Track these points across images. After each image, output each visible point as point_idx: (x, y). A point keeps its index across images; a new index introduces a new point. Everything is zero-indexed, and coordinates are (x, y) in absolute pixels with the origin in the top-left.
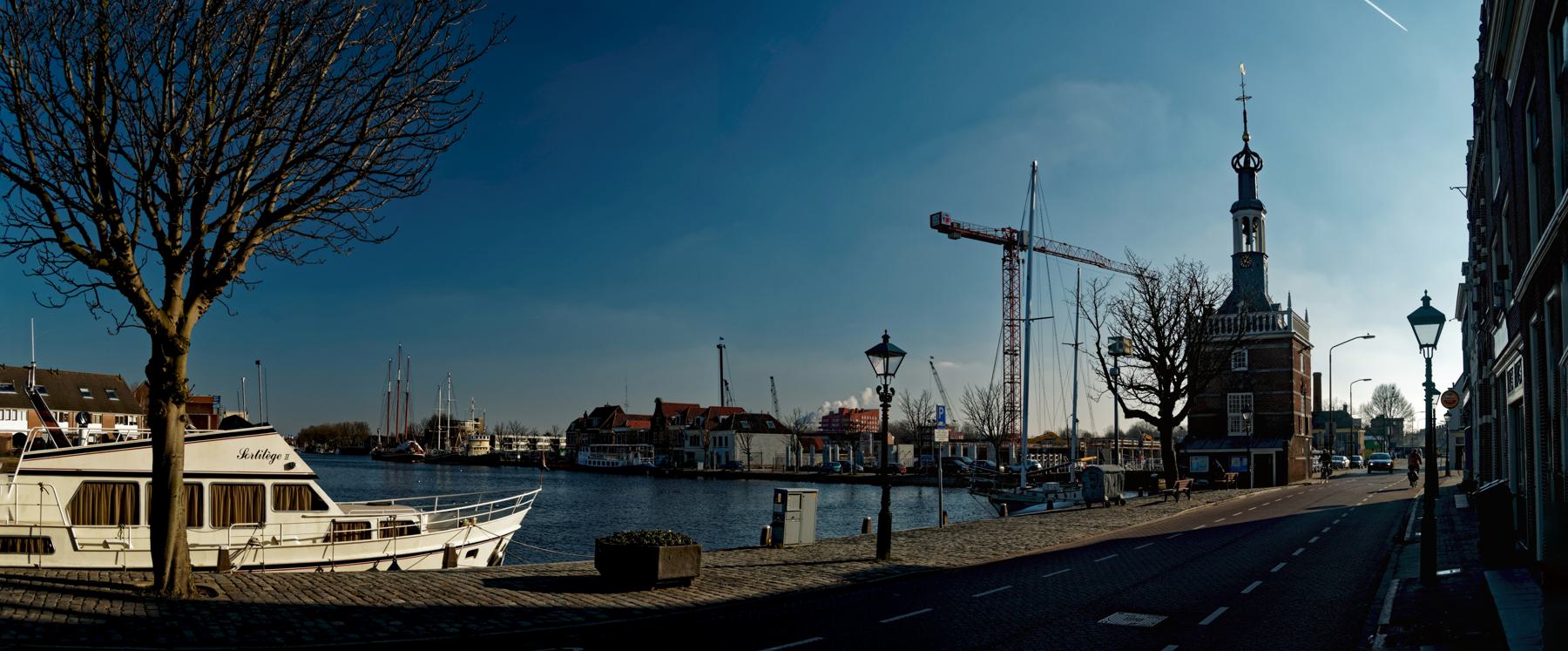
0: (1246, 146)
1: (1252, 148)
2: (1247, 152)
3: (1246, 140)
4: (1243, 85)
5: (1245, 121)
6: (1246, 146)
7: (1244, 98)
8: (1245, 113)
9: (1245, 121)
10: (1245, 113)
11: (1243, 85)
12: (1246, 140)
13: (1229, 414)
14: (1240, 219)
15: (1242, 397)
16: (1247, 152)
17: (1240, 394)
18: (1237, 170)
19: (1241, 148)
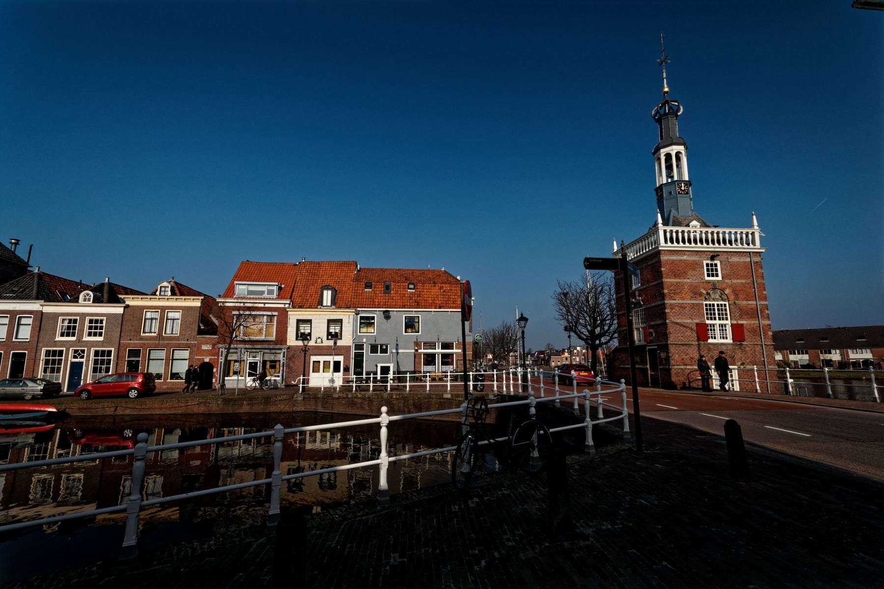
15: (718, 305)
17: (716, 303)
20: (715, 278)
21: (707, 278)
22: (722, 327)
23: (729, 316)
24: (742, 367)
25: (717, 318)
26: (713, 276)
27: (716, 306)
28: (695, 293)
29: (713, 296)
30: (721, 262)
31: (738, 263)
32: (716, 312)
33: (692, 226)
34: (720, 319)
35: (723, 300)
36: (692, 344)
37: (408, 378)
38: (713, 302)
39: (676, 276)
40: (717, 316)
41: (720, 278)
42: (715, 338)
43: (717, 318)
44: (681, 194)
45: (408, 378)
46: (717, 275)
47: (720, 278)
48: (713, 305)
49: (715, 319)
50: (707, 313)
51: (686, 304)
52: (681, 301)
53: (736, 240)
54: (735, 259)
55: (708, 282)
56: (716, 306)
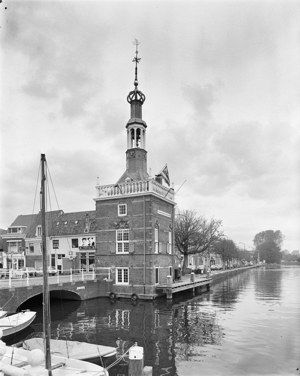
0: (136, 88)
1: (139, 88)
2: (136, 92)
3: (136, 84)
4: (137, 52)
5: (136, 74)
7: (137, 60)
8: (136, 69)
9: (136, 74)
10: (136, 69)
11: (137, 52)
12: (136, 84)
13: (117, 242)
14: (129, 130)
15: (124, 231)
16: (136, 92)
17: (123, 230)
18: (131, 102)
19: (133, 88)
21: (119, 215)
24: (131, 268)
25: (123, 239)
26: (122, 214)
27: (123, 231)
28: (111, 225)
29: (121, 226)
30: (127, 204)
31: (137, 203)
33: (127, 181)
34: (124, 240)
35: (127, 228)
36: (107, 255)
39: (102, 216)
40: (123, 238)
41: (126, 215)
42: (122, 251)
43: (123, 239)
49: (121, 240)
50: (128, 236)
51: (106, 232)
52: (103, 230)
54: (134, 202)
55: (119, 218)
56: (123, 231)
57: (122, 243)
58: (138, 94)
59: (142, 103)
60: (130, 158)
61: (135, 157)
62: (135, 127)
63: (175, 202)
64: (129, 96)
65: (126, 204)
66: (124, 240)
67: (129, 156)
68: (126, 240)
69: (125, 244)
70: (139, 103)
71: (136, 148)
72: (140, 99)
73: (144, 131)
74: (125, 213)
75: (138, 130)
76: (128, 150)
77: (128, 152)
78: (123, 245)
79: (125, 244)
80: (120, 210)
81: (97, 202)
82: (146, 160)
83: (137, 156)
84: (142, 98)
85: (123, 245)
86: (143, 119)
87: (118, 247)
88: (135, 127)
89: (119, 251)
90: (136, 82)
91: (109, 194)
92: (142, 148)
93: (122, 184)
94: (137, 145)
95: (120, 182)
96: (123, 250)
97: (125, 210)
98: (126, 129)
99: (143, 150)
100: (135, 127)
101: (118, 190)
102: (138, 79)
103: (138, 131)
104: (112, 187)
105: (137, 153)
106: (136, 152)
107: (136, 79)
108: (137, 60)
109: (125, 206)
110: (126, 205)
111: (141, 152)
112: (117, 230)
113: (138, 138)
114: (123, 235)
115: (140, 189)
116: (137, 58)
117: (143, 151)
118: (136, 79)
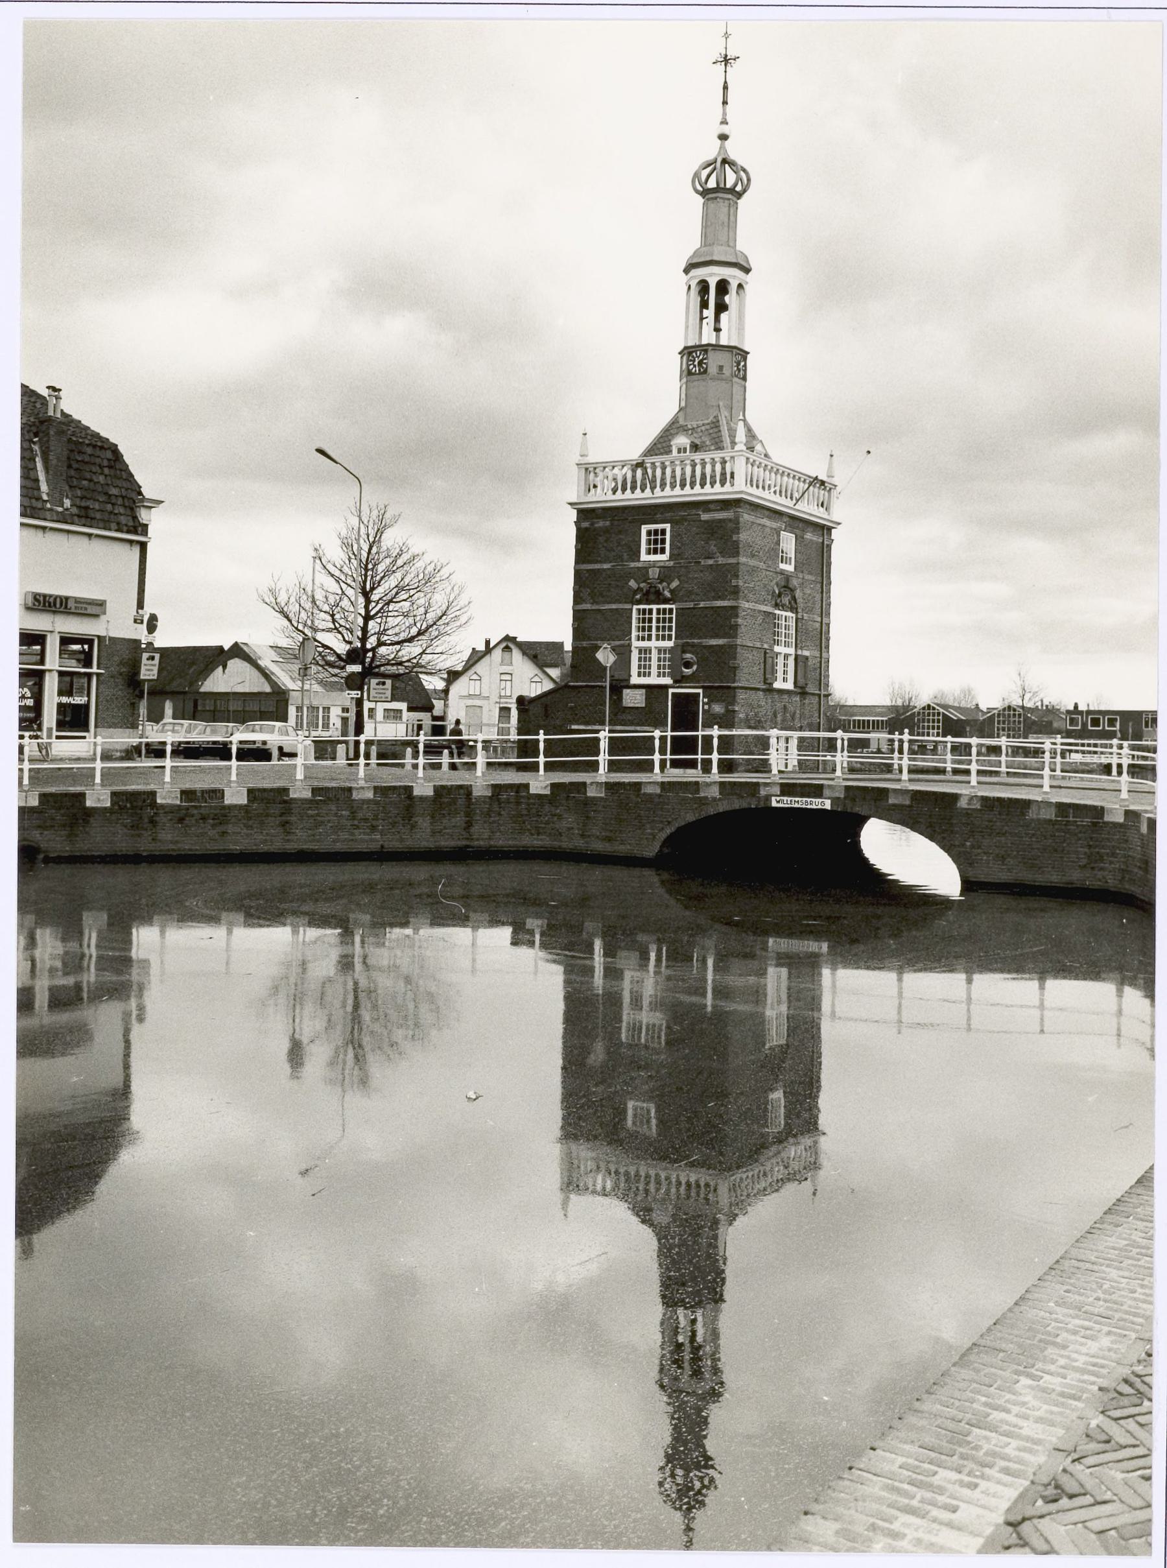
1: (734, 151)
6: (722, 147)
7: (726, 60)
8: (725, 88)
13: (636, 644)
14: (694, 283)
15: (658, 611)
18: (705, 193)
19: (711, 150)
20: (659, 557)
22: (645, 654)
23: (673, 633)
25: (654, 637)
27: (655, 612)
32: (654, 624)
34: (658, 639)
37: (542, 746)
38: (651, 607)
44: (695, 374)
45: (542, 746)
46: (649, 552)
47: (665, 557)
48: (651, 611)
53: (713, 477)
56: (655, 612)
57: (650, 651)
58: (727, 165)
59: (739, 195)
60: (690, 373)
61: (705, 371)
62: (711, 275)
63: (834, 519)
64: (697, 175)
65: (669, 525)
66: (658, 639)
67: (688, 366)
68: (663, 639)
69: (659, 650)
70: (730, 196)
71: (714, 342)
72: (736, 185)
73: (740, 286)
74: (663, 551)
75: (723, 287)
76: (686, 348)
77: (688, 352)
78: (654, 655)
79: (659, 650)
80: (649, 542)
81: (580, 511)
82: (744, 379)
83: (713, 370)
84: (739, 179)
85: (654, 655)
86: (740, 246)
87: (637, 663)
88: (711, 275)
89: (639, 675)
90: (725, 129)
91: (614, 491)
92: (732, 344)
93: (657, 460)
94: (717, 330)
95: (652, 451)
96: (654, 670)
97: (663, 541)
98: (684, 278)
99: (735, 347)
100: (713, 275)
101: (644, 479)
102: (729, 119)
103: (723, 287)
104: (625, 469)
105: (714, 361)
106: (711, 354)
107: (724, 122)
108: (726, 60)
109: (663, 532)
110: (668, 527)
111: (727, 355)
112: (635, 607)
113: (721, 308)
114: (654, 624)
115: (721, 480)
116: (726, 56)
117: (734, 350)
118: (724, 122)
